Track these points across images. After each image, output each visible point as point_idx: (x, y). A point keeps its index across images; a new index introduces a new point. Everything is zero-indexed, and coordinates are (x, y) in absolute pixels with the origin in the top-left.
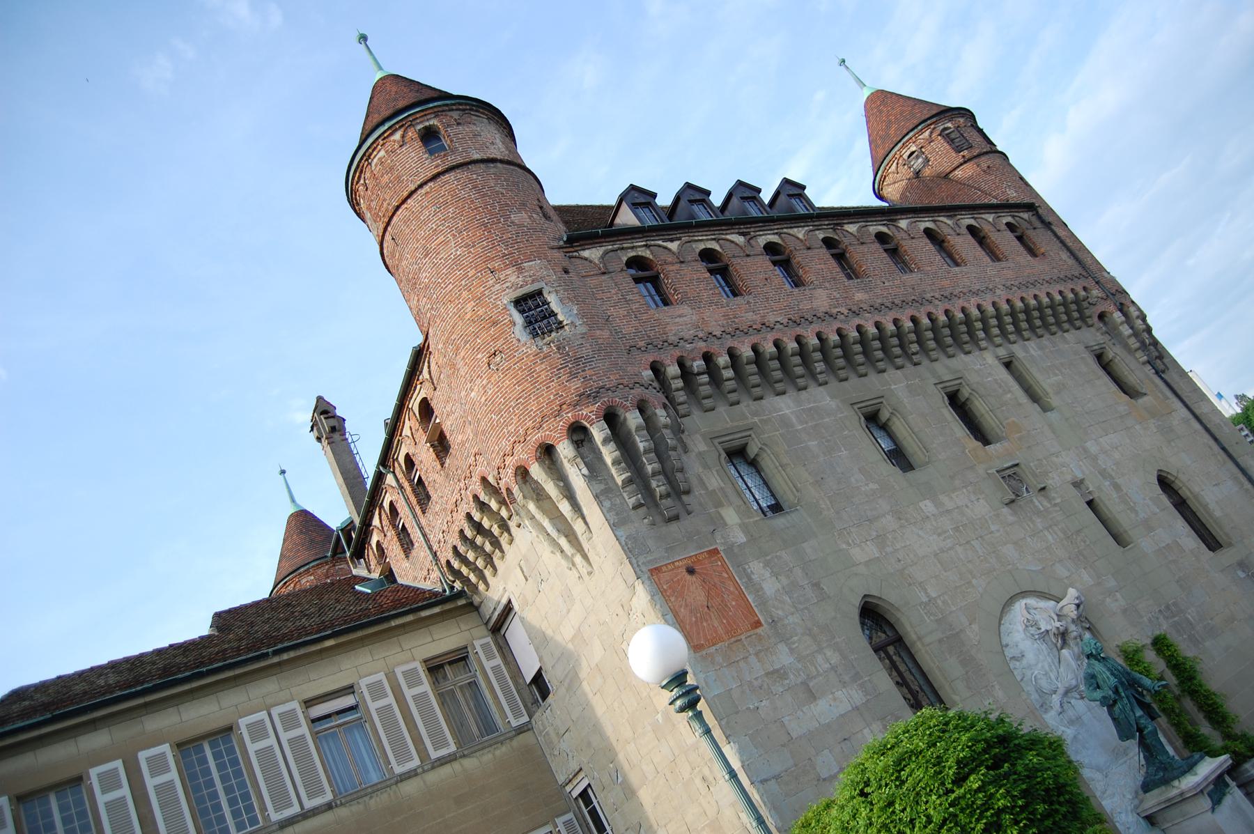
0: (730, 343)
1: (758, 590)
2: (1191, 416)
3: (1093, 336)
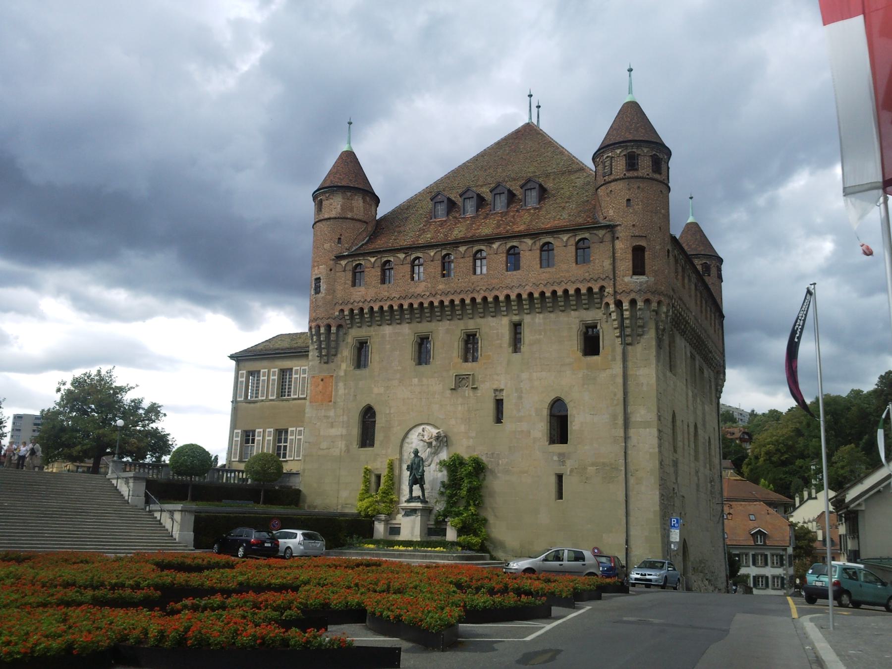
1: (337, 391)
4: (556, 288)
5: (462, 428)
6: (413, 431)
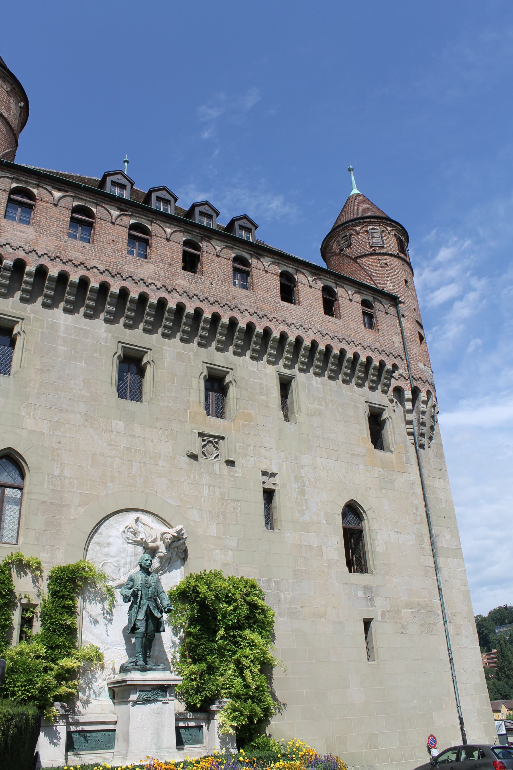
0: (45, 261)
2: (420, 483)
3: (379, 398)
4: (346, 348)
5: (213, 530)
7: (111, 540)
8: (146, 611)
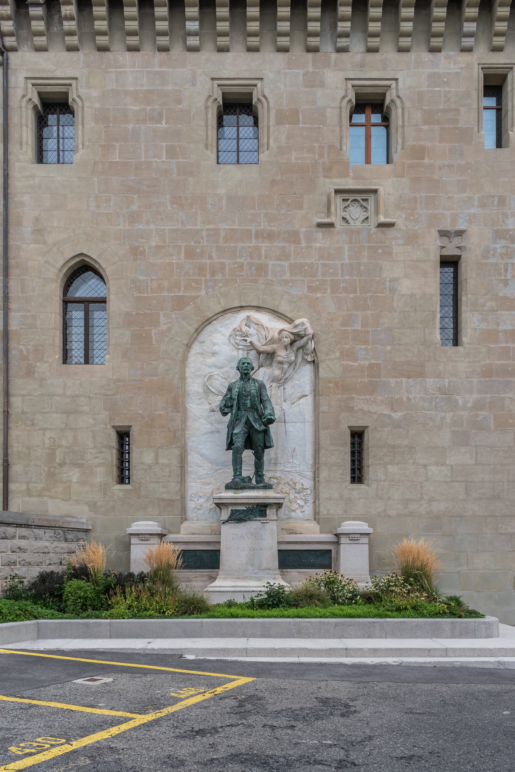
6: (216, 325)
7: (216, 348)
8: (246, 423)
